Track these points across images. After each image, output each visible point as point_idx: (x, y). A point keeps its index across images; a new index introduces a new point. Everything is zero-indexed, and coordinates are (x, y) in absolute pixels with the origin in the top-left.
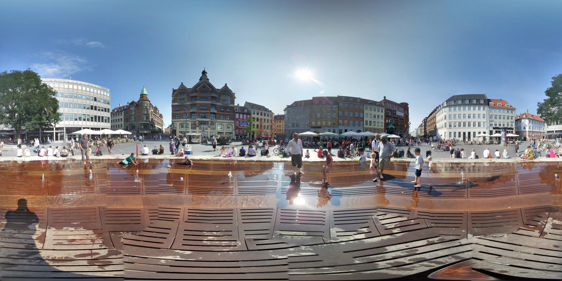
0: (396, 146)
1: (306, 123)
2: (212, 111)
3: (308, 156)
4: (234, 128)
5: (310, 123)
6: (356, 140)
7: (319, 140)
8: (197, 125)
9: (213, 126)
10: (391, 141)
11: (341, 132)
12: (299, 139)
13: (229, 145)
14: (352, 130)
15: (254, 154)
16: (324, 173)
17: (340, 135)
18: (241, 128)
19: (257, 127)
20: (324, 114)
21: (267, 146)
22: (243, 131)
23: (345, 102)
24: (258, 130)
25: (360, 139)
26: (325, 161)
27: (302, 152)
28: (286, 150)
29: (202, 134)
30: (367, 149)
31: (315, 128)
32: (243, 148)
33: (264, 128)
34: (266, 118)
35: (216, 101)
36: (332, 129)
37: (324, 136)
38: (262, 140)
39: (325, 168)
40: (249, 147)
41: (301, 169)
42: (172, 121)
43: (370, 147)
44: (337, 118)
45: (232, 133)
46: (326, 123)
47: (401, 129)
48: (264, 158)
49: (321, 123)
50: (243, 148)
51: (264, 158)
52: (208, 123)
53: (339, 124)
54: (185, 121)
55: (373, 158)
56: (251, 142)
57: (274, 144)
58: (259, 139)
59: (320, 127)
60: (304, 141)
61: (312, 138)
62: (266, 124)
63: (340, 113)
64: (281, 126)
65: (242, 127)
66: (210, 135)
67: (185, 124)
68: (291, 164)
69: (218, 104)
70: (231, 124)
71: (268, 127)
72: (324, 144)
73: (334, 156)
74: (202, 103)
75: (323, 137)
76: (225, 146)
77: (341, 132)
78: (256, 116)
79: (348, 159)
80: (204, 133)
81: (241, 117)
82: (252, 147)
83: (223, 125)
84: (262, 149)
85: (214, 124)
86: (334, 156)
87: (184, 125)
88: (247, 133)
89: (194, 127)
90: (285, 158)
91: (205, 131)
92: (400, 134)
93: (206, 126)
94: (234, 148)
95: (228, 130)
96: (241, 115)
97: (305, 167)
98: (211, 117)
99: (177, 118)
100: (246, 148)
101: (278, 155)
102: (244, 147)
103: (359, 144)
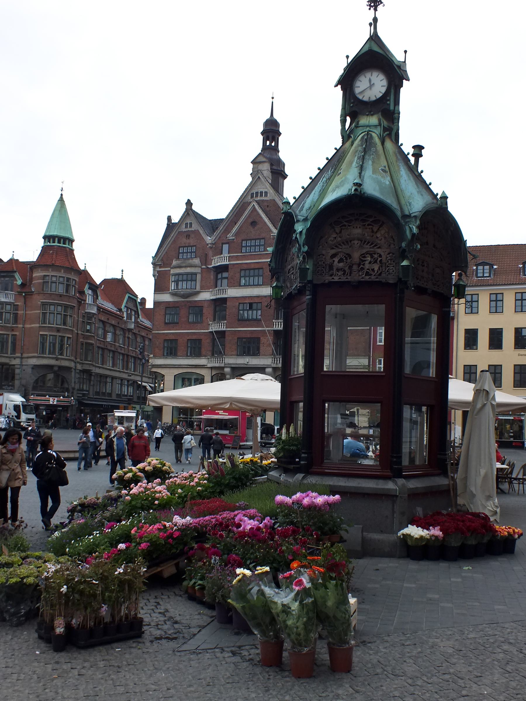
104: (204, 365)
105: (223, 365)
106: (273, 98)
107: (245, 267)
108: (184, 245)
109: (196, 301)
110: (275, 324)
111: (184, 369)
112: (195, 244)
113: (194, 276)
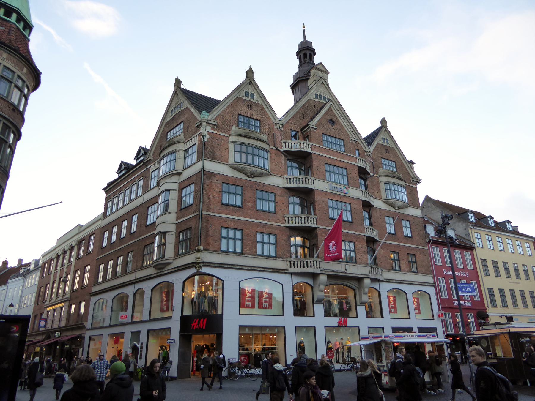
104: (285, 270)
105: (318, 271)
106: (304, 27)
107: (329, 161)
108: (246, 115)
109: (264, 185)
110: (366, 229)
111: (253, 272)
112: (259, 119)
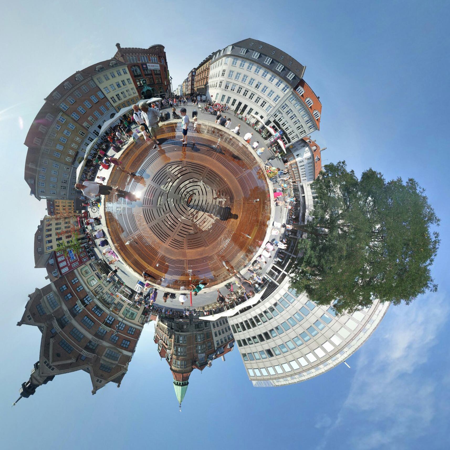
0: (160, 110)
1: (65, 169)
2: (83, 307)
3: (104, 179)
4: (83, 266)
5: (66, 163)
6: (117, 126)
7: (92, 161)
8: (114, 305)
9: (98, 291)
10: (153, 106)
11: (97, 134)
12: (83, 184)
13: (104, 260)
14: (105, 121)
15: (101, 231)
16: (123, 171)
17: (100, 136)
18: (79, 256)
19: (70, 236)
20: (62, 139)
21: (90, 220)
22: (81, 253)
23: (65, 97)
24: (73, 235)
25: (119, 122)
26: (114, 165)
27: (97, 183)
28: (93, 200)
29: (116, 292)
30: (133, 126)
31: (76, 159)
32: (99, 245)
33: (69, 227)
34: (53, 227)
35: (64, 315)
36: (87, 141)
37: (89, 154)
38: (84, 227)
39: (120, 168)
40: (96, 238)
41: (113, 188)
42: (142, 327)
43: (134, 122)
44: (78, 125)
45: (90, 264)
46: (76, 143)
47: (160, 88)
48: (103, 221)
49: (72, 149)
50: (99, 245)
51: (103, 221)
52: (101, 298)
53: (87, 129)
54: (125, 320)
55: (143, 130)
56: (90, 239)
57: (87, 212)
58: (84, 231)
59: (77, 153)
60: (86, 178)
61: (86, 168)
62: (63, 226)
63: (73, 117)
64: (64, 205)
65: (77, 256)
66: (109, 284)
67: (128, 316)
68: (107, 196)
69: (65, 308)
70: (80, 272)
71: (66, 223)
72: (98, 158)
73: (114, 155)
74: (86, 329)
75: (90, 155)
76: (108, 263)
77: (97, 132)
78: (54, 244)
79: (125, 147)
80: (112, 291)
81: (64, 263)
82: (95, 235)
83: (88, 280)
84: (95, 225)
85: (95, 291)
86: (114, 155)
87: (130, 316)
88: (82, 247)
89: (118, 307)
90: (102, 201)
91: (110, 293)
92: (161, 95)
93: (106, 297)
94: (104, 254)
95: (89, 271)
96: (61, 265)
97: (112, 184)
98: (90, 301)
99: (134, 330)
100: (98, 242)
101: (98, 208)
102: (98, 245)
103: (122, 128)
109: (111, 344)
113: (106, 355)
